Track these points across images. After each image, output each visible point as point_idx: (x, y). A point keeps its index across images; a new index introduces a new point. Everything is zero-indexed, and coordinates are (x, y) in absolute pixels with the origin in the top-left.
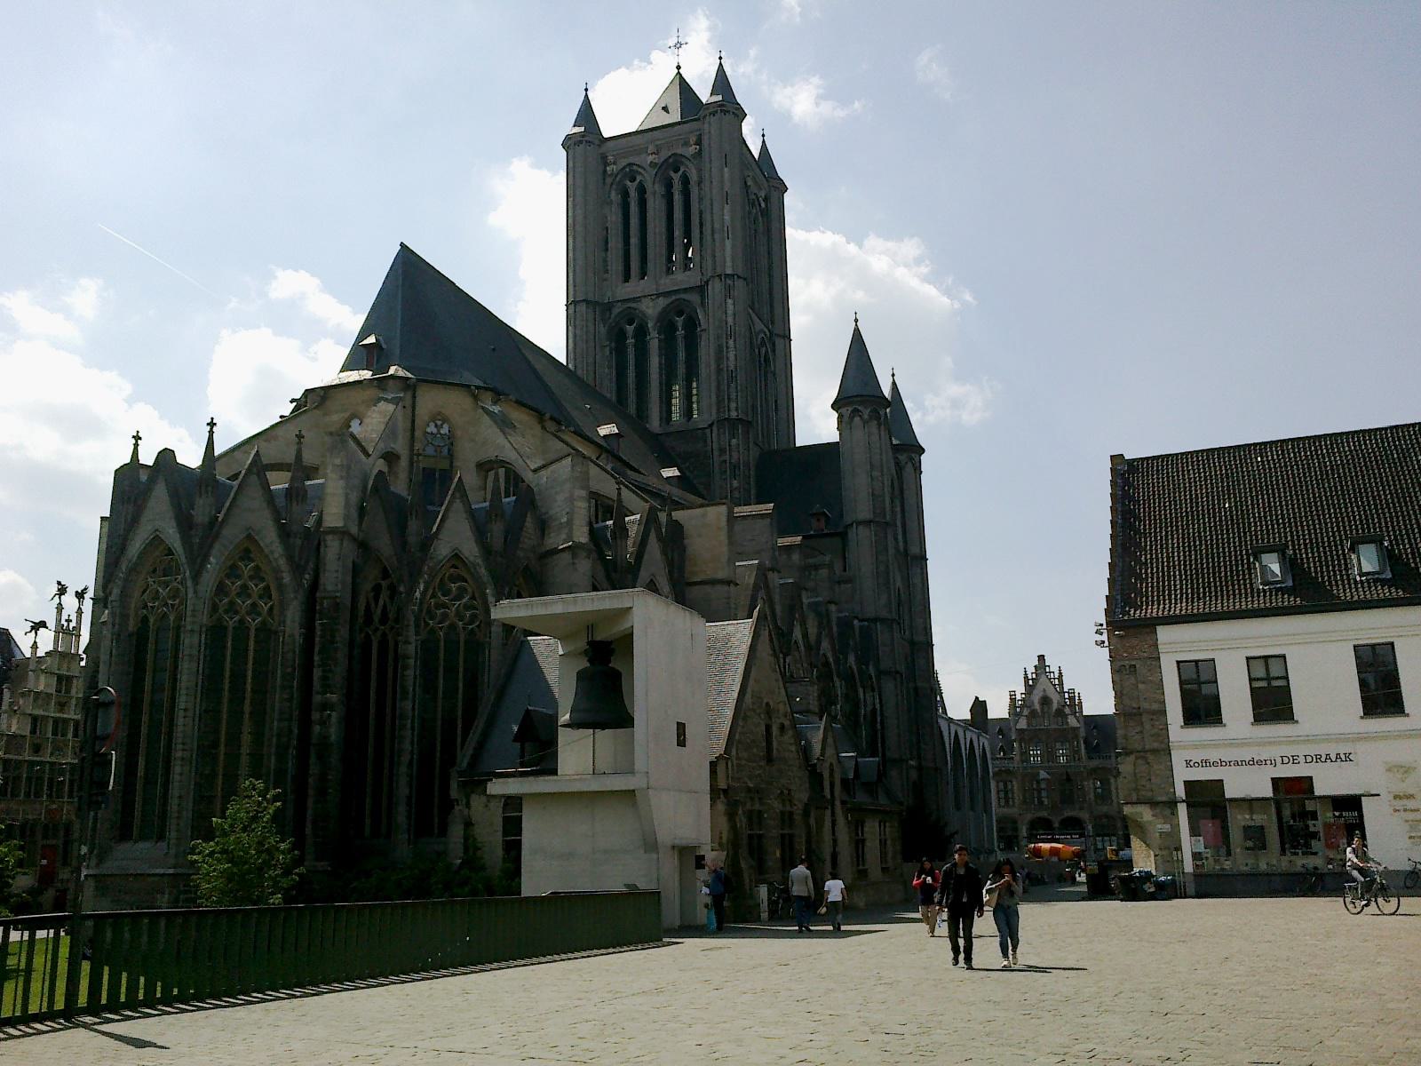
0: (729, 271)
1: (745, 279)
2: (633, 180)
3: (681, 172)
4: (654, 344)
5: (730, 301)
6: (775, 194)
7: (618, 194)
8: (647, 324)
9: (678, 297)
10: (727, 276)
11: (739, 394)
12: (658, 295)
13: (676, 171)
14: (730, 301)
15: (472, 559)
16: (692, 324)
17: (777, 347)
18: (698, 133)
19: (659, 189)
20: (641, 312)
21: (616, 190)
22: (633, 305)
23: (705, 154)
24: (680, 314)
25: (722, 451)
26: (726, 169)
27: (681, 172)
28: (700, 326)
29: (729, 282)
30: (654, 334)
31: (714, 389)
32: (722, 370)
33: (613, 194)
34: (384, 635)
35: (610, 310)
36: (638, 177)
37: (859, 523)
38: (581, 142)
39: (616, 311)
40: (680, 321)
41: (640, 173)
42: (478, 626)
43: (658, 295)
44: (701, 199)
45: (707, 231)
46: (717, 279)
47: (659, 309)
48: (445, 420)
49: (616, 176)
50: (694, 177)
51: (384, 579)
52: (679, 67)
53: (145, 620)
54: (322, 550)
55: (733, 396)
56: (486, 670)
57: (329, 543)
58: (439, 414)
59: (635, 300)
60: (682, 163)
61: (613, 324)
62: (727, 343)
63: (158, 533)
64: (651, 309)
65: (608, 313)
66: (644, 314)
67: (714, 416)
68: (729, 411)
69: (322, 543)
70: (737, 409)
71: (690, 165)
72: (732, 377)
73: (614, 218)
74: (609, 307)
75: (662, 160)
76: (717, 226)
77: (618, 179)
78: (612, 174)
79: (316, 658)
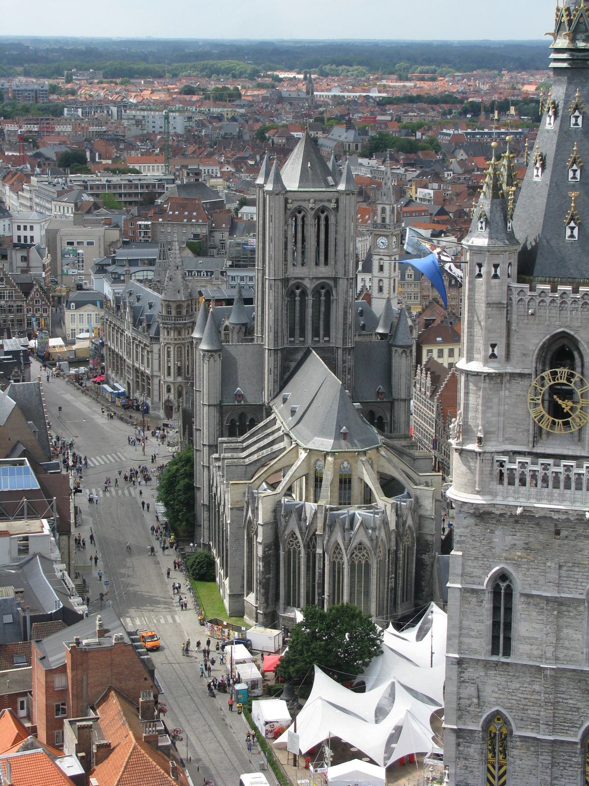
3: (325, 214)
4: (310, 300)
9: (323, 281)
12: (313, 278)
13: (323, 212)
16: (328, 294)
24: (323, 288)
25: (344, 362)
32: (346, 324)
37: (402, 400)
39: (292, 282)
40: (323, 291)
44: (336, 232)
45: (340, 253)
46: (345, 280)
47: (313, 286)
50: (332, 220)
53: (353, 562)
59: (301, 278)
64: (309, 285)
66: (306, 287)
75: (317, 208)
76: (347, 253)
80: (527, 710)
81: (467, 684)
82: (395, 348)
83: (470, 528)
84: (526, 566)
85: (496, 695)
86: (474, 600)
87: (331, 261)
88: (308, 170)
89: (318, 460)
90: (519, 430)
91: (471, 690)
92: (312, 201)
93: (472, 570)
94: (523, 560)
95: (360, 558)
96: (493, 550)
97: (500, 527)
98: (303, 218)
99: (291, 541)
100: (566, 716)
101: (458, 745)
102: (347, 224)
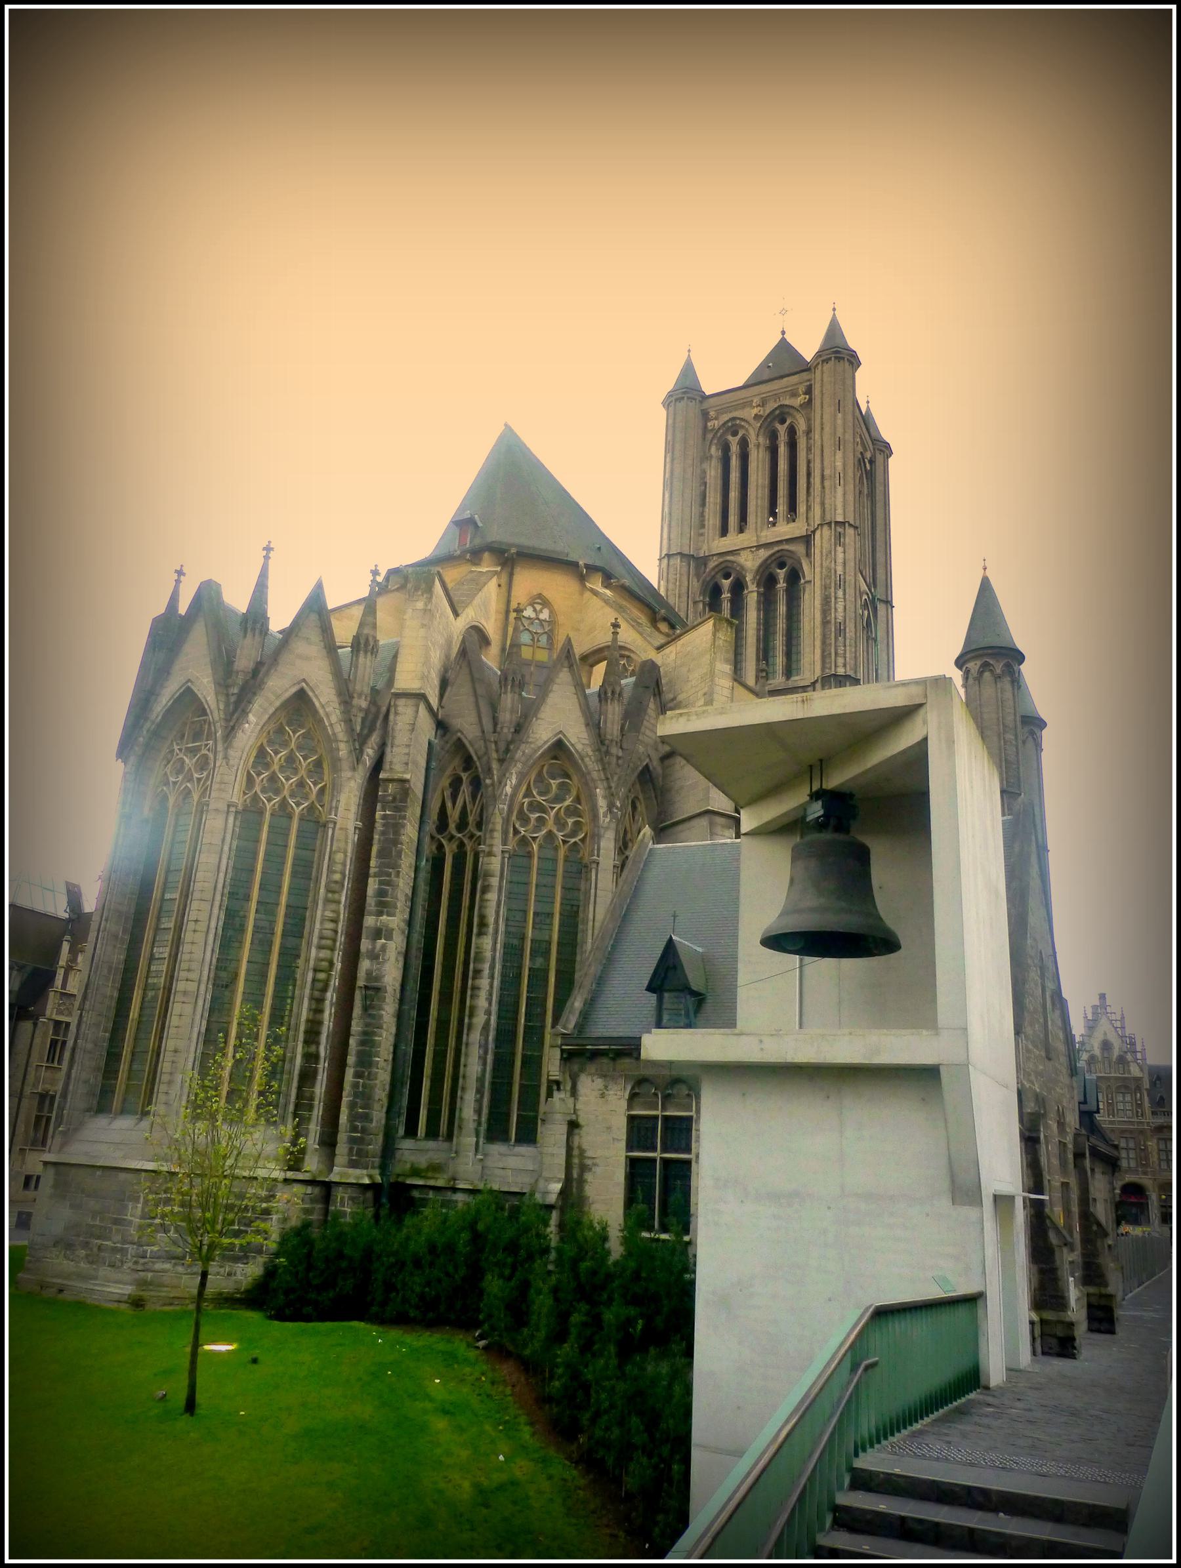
0: (840, 519)
1: (856, 528)
4: (752, 597)
5: (840, 549)
6: (879, 458)
7: (718, 449)
8: (745, 577)
10: (836, 523)
11: (848, 648)
12: (759, 547)
13: (783, 422)
14: (840, 549)
15: (579, 747)
16: (794, 577)
17: (879, 613)
18: (808, 383)
19: (763, 441)
20: (739, 565)
21: (716, 444)
23: (817, 402)
24: (782, 565)
26: (840, 415)
27: (788, 423)
28: (804, 578)
29: (839, 529)
30: (752, 587)
31: (818, 643)
32: (829, 622)
33: (713, 449)
34: (462, 845)
35: (705, 565)
38: (683, 398)
39: (712, 564)
40: (781, 574)
41: (743, 427)
42: (583, 840)
43: (759, 547)
45: (816, 480)
46: (826, 528)
47: (759, 562)
48: (546, 603)
49: (717, 431)
51: (465, 769)
52: (783, 333)
54: (391, 717)
55: (840, 651)
56: (592, 898)
57: (400, 709)
58: (540, 596)
60: (788, 413)
61: (708, 579)
62: (835, 593)
63: (189, 684)
64: (750, 563)
65: (703, 567)
66: (742, 567)
67: (818, 673)
68: (836, 666)
69: (392, 710)
70: (845, 666)
71: (798, 416)
72: (840, 631)
73: (713, 473)
75: (768, 412)
76: (827, 472)
77: (719, 434)
78: (712, 430)
79: (373, 863)
82: (964, 668)
87: (801, 508)
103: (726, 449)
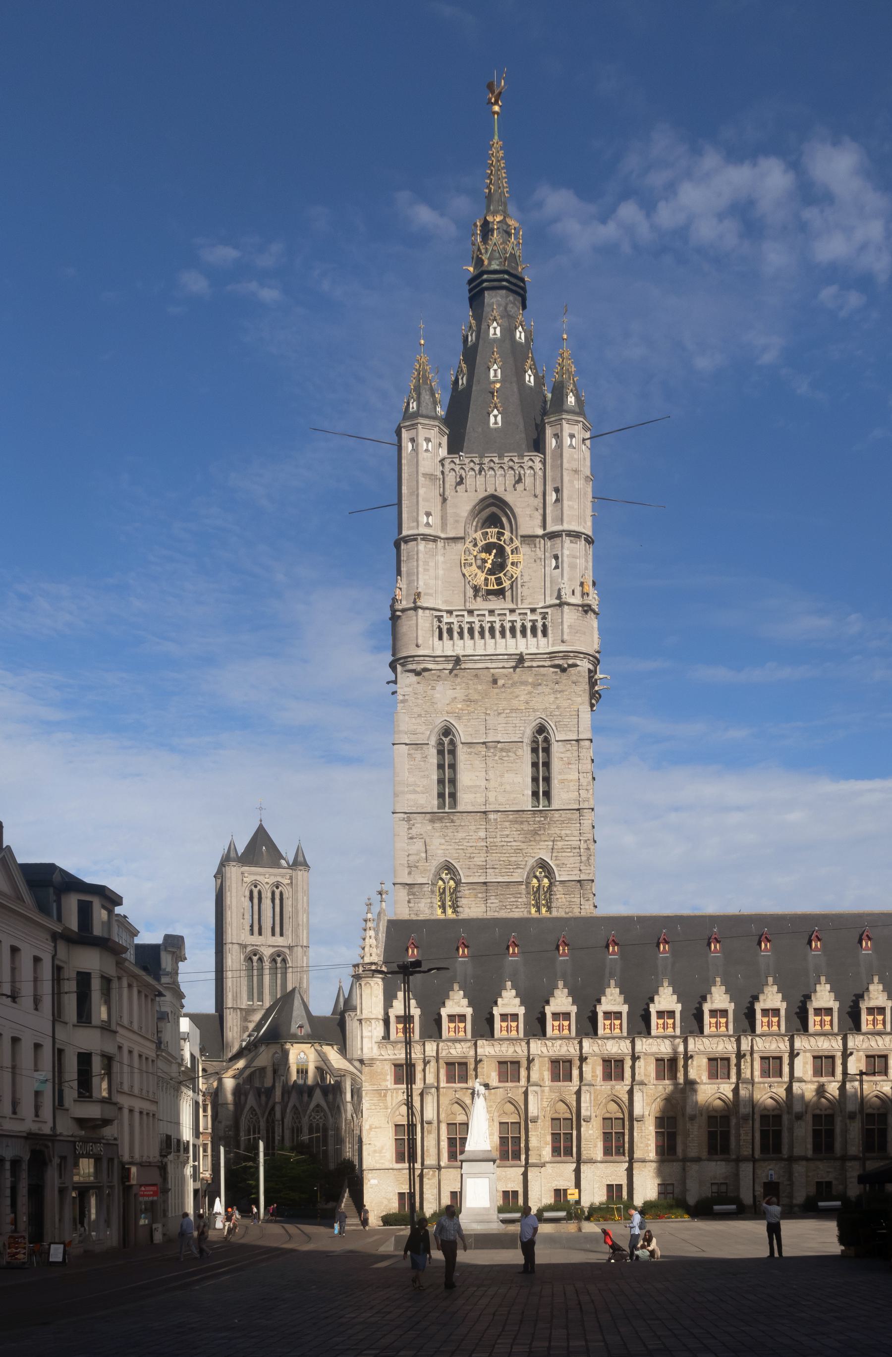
0: (305, 944)
2: (256, 887)
3: (280, 888)
5: (305, 958)
10: (305, 946)
12: (269, 946)
13: (277, 888)
16: (284, 961)
19: (269, 895)
22: (255, 947)
24: (279, 956)
29: (305, 949)
36: (258, 886)
39: (249, 949)
40: (279, 960)
43: (269, 946)
46: (299, 948)
52: (261, 821)
53: (311, 1124)
64: (267, 952)
66: (263, 953)
74: (245, 946)
80: (474, 857)
81: (415, 840)
82: (348, 1013)
83: (412, 686)
84: (467, 718)
85: (443, 847)
86: (418, 755)
88: (262, 853)
89: (276, 1053)
90: (456, 592)
91: (419, 845)
92: (267, 876)
93: (415, 727)
94: (464, 712)
95: (318, 1120)
96: (435, 706)
97: (441, 683)
98: (260, 893)
99: (251, 1118)
100: (510, 859)
101: (409, 902)
102: (300, 897)
103: (251, 892)
